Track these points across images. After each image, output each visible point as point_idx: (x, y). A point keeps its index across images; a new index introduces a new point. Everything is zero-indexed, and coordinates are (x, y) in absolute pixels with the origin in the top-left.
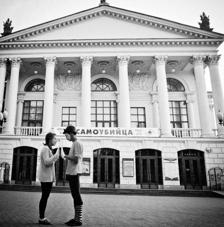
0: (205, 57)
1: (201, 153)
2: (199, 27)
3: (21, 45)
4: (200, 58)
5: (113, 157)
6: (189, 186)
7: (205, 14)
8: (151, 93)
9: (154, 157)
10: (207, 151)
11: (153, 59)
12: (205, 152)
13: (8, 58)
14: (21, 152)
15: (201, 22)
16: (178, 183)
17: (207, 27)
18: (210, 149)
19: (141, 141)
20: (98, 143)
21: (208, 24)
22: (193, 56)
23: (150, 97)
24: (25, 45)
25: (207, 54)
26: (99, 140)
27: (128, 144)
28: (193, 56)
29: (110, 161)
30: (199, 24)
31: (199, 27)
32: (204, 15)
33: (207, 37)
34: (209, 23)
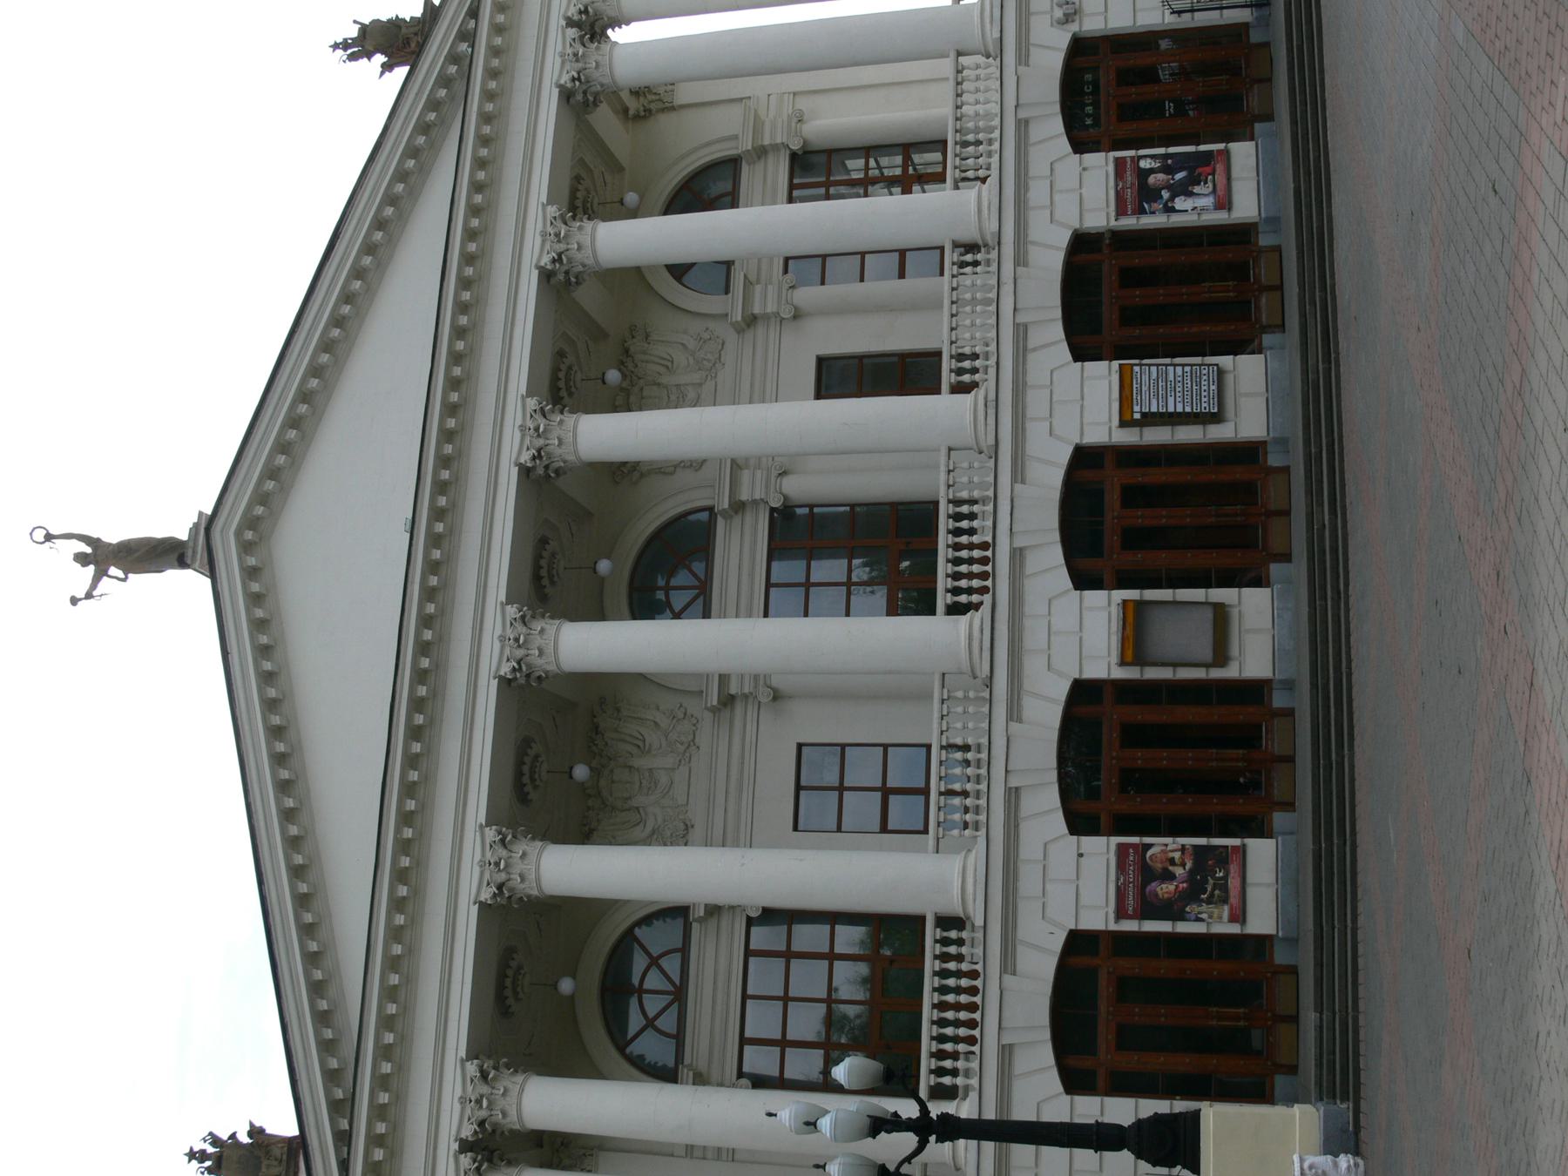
0: (572, 32)
1: (1081, 50)
2: (407, 68)
3: (384, 1052)
4: (576, 55)
5: (1113, 482)
6: (1253, 102)
7: (340, 40)
8: (738, 316)
10: (1067, 19)
11: (553, 281)
12: (1075, 27)
13: (456, 1146)
15: (380, 59)
16: (1243, 154)
17: (413, 30)
18: (1060, 6)
19: (1021, 331)
21: (396, 24)
22: (561, 87)
23: (760, 330)
24: (387, 1022)
25: (557, 21)
26: (1012, 558)
27: (1036, 403)
28: (561, 87)
29: (1131, 496)
30: (387, 68)
31: (407, 68)
32: (345, 45)
33: (472, 23)
34: (390, 21)
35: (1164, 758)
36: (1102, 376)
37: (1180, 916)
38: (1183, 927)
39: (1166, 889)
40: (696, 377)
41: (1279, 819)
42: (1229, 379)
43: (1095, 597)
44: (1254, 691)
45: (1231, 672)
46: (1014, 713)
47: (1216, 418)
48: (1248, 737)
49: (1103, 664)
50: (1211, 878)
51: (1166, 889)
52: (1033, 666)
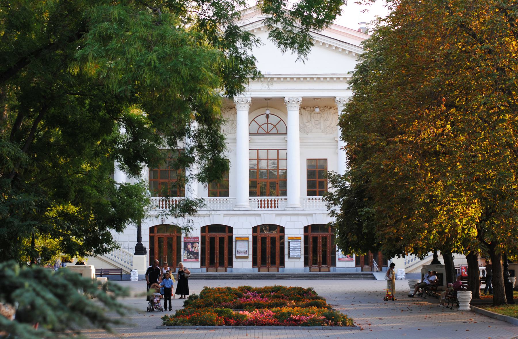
9: (327, 233)
14: (209, 232)
19: (311, 215)
20: (258, 218)
27: (294, 218)
35: (217, 246)
36: (301, 233)
37: (184, 250)
38: (182, 250)
39: (190, 246)
40: (322, 127)
41: (204, 269)
42: (298, 260)
43: (250, 232)
44: (231, 264)
45: (234, 259)
46: (225, 215)
47: (289, 257)
48: (221, 263)
49: (236, 234)
50: (193, 255)
51: (190, 246)
52: (236, 219)
